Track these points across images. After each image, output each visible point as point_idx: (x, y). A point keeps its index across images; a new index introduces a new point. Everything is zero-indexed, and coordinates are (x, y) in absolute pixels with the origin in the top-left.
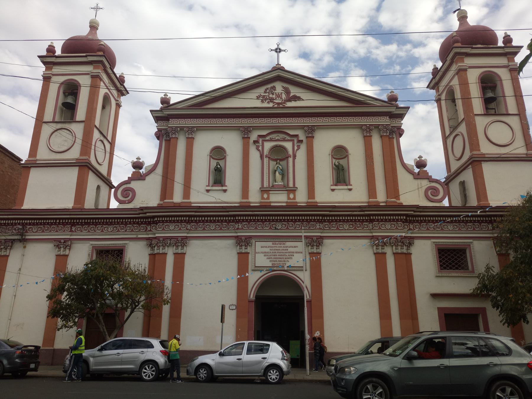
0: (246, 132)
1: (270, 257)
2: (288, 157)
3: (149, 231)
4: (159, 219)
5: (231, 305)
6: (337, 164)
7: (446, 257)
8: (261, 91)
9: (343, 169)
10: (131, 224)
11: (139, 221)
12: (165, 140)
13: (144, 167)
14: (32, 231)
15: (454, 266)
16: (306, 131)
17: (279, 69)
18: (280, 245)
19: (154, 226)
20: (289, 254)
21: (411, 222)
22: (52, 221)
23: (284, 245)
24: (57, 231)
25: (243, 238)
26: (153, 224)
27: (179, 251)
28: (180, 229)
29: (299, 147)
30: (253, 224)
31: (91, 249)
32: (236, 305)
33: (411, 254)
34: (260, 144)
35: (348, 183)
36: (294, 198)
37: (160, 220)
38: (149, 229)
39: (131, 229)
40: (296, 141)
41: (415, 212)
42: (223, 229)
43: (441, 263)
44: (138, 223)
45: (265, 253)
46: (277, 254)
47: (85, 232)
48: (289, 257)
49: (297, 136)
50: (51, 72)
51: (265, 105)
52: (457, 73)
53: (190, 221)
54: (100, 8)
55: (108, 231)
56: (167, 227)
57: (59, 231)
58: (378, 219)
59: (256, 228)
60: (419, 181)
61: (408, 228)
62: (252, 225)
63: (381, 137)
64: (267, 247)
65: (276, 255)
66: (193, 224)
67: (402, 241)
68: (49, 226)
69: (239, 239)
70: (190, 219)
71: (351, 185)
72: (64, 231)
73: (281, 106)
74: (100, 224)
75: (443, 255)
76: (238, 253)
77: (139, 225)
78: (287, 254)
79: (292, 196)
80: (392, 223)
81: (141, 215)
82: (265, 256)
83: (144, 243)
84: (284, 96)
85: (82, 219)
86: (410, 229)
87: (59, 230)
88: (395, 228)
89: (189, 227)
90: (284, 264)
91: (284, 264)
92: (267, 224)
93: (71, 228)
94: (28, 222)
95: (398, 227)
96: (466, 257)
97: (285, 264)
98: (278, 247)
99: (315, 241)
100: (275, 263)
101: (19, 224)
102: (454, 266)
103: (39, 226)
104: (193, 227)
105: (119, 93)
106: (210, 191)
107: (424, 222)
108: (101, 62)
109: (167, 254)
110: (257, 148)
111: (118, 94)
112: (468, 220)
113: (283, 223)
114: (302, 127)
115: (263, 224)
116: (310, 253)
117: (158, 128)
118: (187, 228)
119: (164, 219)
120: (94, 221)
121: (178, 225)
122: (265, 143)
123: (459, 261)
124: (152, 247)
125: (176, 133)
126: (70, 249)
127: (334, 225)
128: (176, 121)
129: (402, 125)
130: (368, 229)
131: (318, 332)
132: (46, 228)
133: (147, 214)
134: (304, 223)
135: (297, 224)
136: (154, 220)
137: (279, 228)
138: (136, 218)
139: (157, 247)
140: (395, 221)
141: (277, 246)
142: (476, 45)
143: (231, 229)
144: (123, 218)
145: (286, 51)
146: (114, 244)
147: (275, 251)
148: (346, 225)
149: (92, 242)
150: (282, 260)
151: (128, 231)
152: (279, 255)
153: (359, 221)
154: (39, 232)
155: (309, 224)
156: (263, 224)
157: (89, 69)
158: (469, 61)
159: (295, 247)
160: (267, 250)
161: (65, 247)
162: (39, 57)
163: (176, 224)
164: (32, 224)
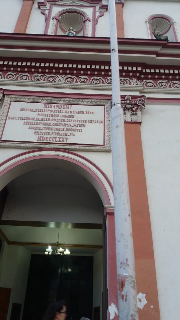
18: (60, 108)
20: (76, 123)
30: (11, 75)
34: (47, 8)
45: (28, 119)
48: (74, 128)
62: (10, 76)
64: (34, 110)
78: (72, 124)
91: (65, 140)
92: (38, 76)
97: (67, 139)
98: (55, 111)
99: (128, 102)
100: (45, 136)
113: (69, 76)
135: (94, 79)
141: (53, 109)
147: (48, 117)
159: (88, 113)
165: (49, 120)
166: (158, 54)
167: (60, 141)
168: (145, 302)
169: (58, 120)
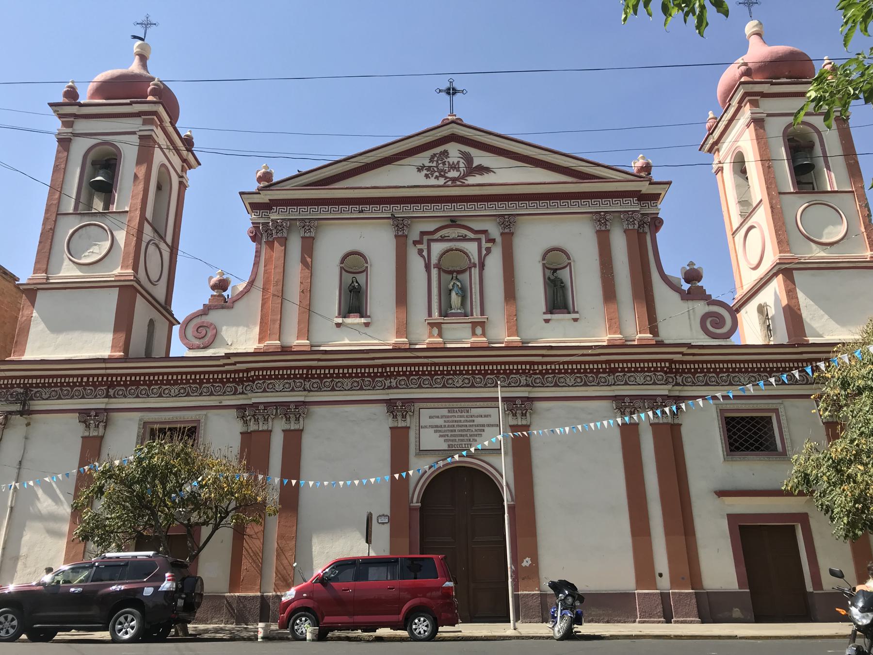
0: (401, 227)
1: (445, 433)
2: (470, 268)
3: (240, 394)
4: (257, 374)
5: (380, 516)
6: (552, 278)
7: (739, 430)
9: (564, 286)
10: (210, 383)
11: (224, 376)
13: (230, 288)
14: (41, 397)
15: (752, 445)
17: (453, 122)
18: (462, 413)
19: (248, 385)
20: (477, 428)
21: (679, 373)
22: (75, 380)
23: (467, 414)
24: (83, 397)
26: (246, 381)
27: (293, 426)
28: (293, 390)
31: (142, 426)
33: (681, 425)
37: (259, 375)
39: (210, 391)
41: (684, 354)
42: (364, 388)
43: (731, 441)
45: (437, 426)
46: (457, 429)
48: (476, 433)
49: (485, 232)
50: (71, 131)
51: (432, 181)
52: (748, 126)
53: (310, 376)
54: (151, 24)
55: (170, 395)
56: (270, 386)
57: (87, 397)
58: (623, 368)
59: (420, 387)
60: (690, 304)
61: (674, 383)
62: (414, 381)
63: (625, 231)
65: (455, 430)
66: (314, 381)
67: (664, 404)
68: (69, 389)
69: (393, 405)
70: (310, 373)
71: (577, 312)
72: (96, 395)
73: (458, 183)
74: (156, 384)
75: (734, 427)
76: (390, 428)
77: (224, 384)
78: (473, 429)
80: (647, 374)
82: (436, 431)
83: (234, 412)
85: (126, 375)
86: (677, 384)
87: (87, 395)
88: (651, 383)
89: (308, 386)
90: (469, 446)
91: (469, 446)
93: (108, 392)
94: (34, 381)
95: (656, 381)
96: (772, 429)
97: (471, 445)
98: (459, 416)
101: (19, 385)
102: (752, 445)
103: (53, 389)
104: (315, 386)
105: (185, 164)
107: (700, 373)
108: (155, 113)
109: (271, 431)
110: (420, 252)
111: (183, 166)
112: (773, 367)
113: (466, 376)
115: (432, 380)
116: (511, 426)
117: (254, 221)
118: (304, 387)
119: (267, 372)
121: (290, 383)
122: (432, 244)
123: (761, 437)
124: (247, 420)
125: (284, 230)
126: (105, 427)
127: (550, 379)
128: (283, 210)
129: (660, 212)
130: (606, 384)
131: (527, 559)
132: (65, 392)
134: (501, 376)
135: (488, 378)
136: (249, 375)
137: (458, 386)
138: (218, 372)
139: (255, 421)
140: (652, 372)
142: (779, 78)
143: (379, 388)
144: (195, 373)
145: (465, 92)
147: (453, 424)
148: (570, 379)
150: (466, 438)
151: (204, 394)
152: (459, 431)
153: (592, 371)
154: (53, 398)
155: (508, 379)
156: (432, 380)
157: (135, 124)
158: (769, 106)
159: (486, 416)
160: (440, 422)
161: (97, 423)
162: (51, 105)
163: (286, 381)
164: (40, 385)
165: (454, 426)
166: (543, 356)
167: (465, 447)
168: (530, 562)
169: (461, 426)
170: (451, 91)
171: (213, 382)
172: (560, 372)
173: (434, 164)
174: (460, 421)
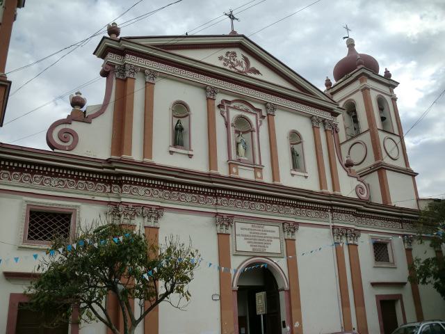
8: (223, 52)
12: (116, 78)
16: (267, 108)
25: (225, 216)
26: (114, 183)
29: (261, 121)
31: (25, 208)
32: (219, 294)
35: (303, 169)
36: (262, 178)
38: (108, 190)
40: (258, 117)
44: (94, 180)
45: (245, 236)
47: (14, 182)
49: (260, 110)
52: (362, 90)
63: (326, 130)
66: (166, 191)
74: (39, 173)
76: (218, 234)
79: (259, 175)
81: (105, 170)
82: (246, 239)
84: (244, 65)
85: (14, 161)
104: (167, 195)
106: (174, 154)
114: (265, 104)
116: (286, 239)
120: (33, 167)
131: (297, 323)
133: (116, 170)
146: (59, 205)
149: (26, 198)
160: (247, 232)
163: (146, 188)
166: (306, 197)
170: (231, 17)
171: (88, 180)
172: (309, 209)
173: (228, 58)
174: (259, 233)
